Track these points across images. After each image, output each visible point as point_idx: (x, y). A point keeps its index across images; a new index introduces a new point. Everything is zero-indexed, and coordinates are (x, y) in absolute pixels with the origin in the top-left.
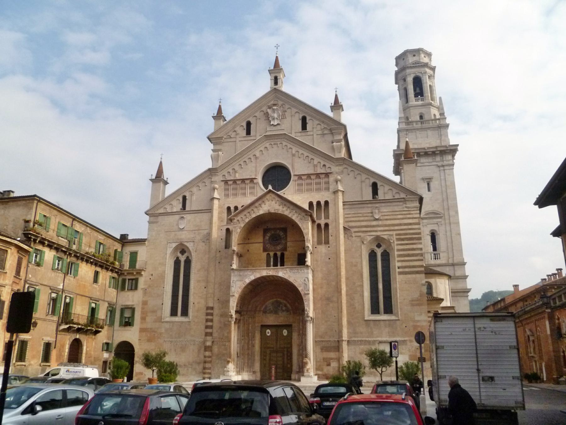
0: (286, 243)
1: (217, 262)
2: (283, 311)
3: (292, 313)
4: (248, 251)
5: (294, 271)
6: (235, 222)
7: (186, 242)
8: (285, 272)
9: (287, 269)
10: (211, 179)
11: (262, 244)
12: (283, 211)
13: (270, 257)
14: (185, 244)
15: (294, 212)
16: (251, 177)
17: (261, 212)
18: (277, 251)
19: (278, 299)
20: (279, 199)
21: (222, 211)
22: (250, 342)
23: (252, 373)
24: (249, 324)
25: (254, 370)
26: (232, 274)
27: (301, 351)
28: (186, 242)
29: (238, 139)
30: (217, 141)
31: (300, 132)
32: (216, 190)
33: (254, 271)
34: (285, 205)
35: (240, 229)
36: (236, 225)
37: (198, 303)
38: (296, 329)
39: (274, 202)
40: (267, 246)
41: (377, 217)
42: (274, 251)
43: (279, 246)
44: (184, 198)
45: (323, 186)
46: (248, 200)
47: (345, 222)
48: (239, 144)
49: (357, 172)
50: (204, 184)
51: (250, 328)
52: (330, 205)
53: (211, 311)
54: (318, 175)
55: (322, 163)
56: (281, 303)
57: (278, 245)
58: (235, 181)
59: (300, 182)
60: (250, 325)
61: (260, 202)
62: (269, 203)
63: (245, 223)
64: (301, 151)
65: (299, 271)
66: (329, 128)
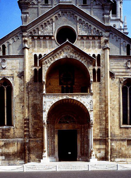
1: (29, 90)
10: (22, 34)
14: (7, 78)
21: (31, 57)
28: (8, 77)
29: (40, 6)
30: (24, 6)
31: (82, 5)
32: (26, 42)
38: (79, 132)
41: (129, 67)
45: (97, 44)
46: (48, 51)
47: (110, 68)
48: (40, 10)
49: (118, 37)
50: (17, 37)
51: (52, 132)
53: (28, 122)
54: (94, 37)
55: (97, 29)
58: (39, 37)
64: (83, 20)
66: (101, 4)
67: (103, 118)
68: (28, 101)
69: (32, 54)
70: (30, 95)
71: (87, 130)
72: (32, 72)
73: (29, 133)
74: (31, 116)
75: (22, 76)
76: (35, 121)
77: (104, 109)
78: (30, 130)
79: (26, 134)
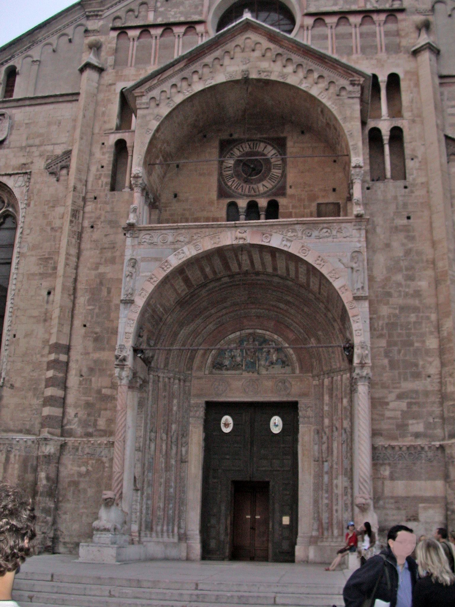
0: (284, 175)
2: (272, 363)
3: (297, 371)
4: (176, 196)
5: (315, 233)
6: (144, 104)
7: (6, 175)
8: (290, 234)
9: (297, 227)
11: (214, 181)
12: (284, 76)
13: (238, 212)
15: (316, 75)
16: (189, 20)
17: (220, 78)
18: (256, 196)
19: (259, 331)
20: (272, 46)
22: (174, 448)
23: (176, 540)
24: (171, 396)
25: (182, 531)
26: (129, 241)
27: (326, 478)
28: (6, 175)
33: (195, 231)
34: (289, 60)
35: (157, 120)
36: (145, 112)
37: (27, 335)
39: (257, 54)
40: (229, 184)
42: (250, 196)
43: (264, 183)
44: (12, 74)
50: (65, 39)
51: (175, 408)
52: (403, 85)
53: (63, 358)
56: (265, 341)
57: (260, 180)
58: (145, 29)
59: (320, 30)
60: (175, 401)
61: (218, 53)
62: (245, 55)
63: (173, 105)
65: (334, 233)
67: (424, 342)
68: (77, 268)
69: (113, 87)
70: (86, 245)
71: (345, 401)
72: (103, 154)
73: (64, 413)
74: (79, 331)
75: (62, 168)
76: (96, 355)
77: (430, 301)
78: (70, 399)
79: (49, 417)
